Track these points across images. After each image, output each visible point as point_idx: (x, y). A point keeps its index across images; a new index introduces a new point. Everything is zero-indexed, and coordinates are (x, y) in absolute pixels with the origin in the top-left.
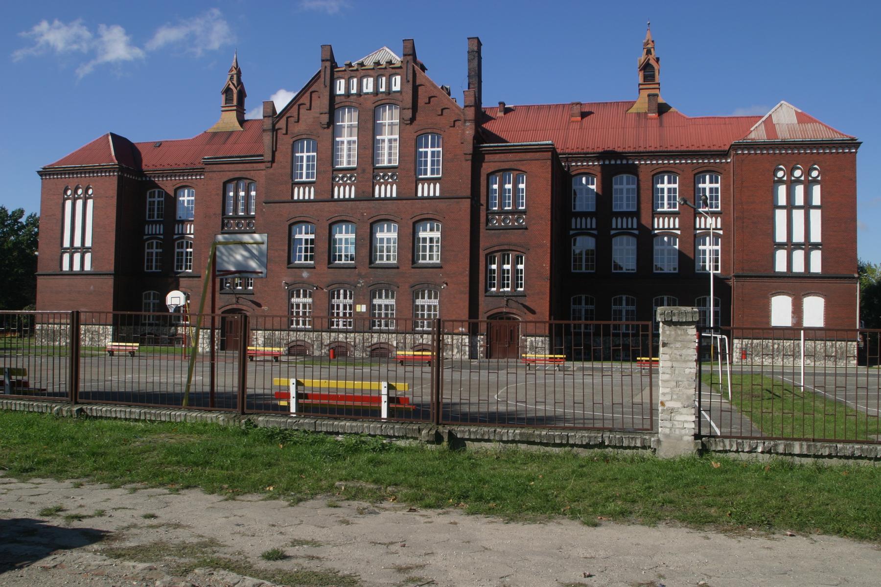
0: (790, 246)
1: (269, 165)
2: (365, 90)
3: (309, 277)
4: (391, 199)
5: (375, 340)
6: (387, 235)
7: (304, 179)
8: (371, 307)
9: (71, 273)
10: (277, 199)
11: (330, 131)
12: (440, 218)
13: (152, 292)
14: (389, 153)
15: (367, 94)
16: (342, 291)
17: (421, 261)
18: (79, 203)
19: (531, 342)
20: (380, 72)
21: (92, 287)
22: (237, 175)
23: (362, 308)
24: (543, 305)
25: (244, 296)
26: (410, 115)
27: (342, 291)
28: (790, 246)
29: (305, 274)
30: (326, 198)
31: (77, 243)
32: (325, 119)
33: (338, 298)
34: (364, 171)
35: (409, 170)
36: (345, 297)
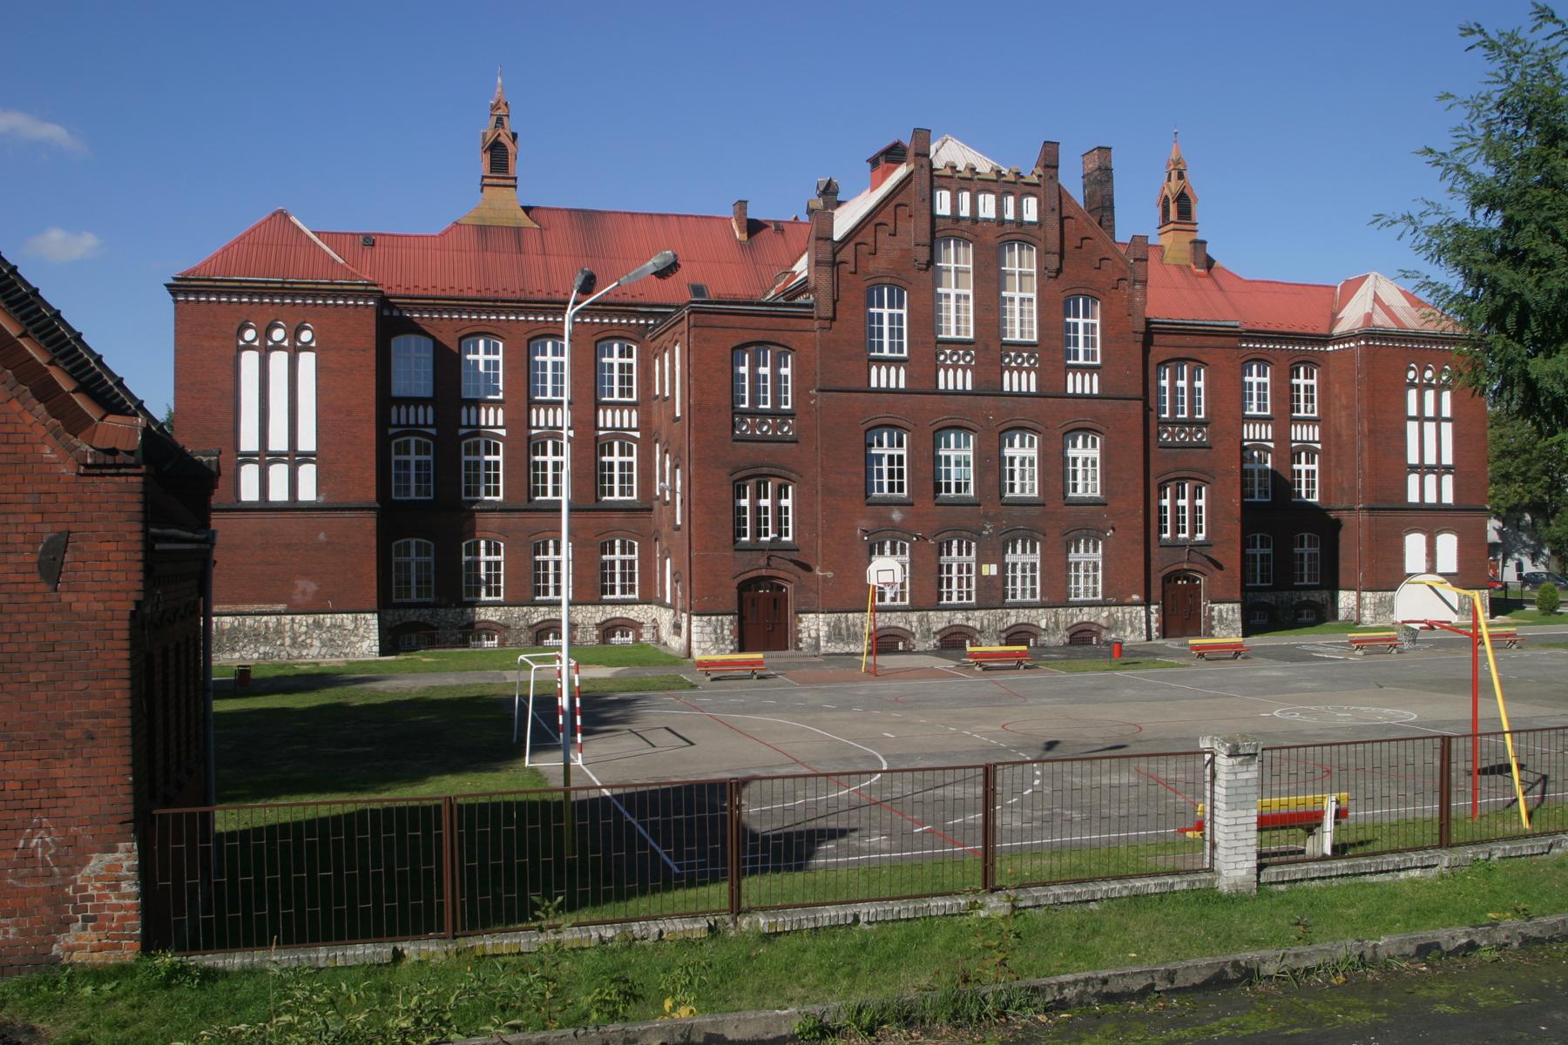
0: (1422, 469)
1: (827, 324)
2: (982, 215)
3: (903, 520)
4: (1028, 395)
5: (1013, 621)
6: (1022, 452)
7: (886, 353)
8: (1003, 568)
9: (264, 506)
10: (842, 384)
11: (927, 276)
12: (1103, 429)
13: (413, 541)
14: (1022, 323)
15: (987, 220)
16: (955, 543)
17: (1071, 494)
18: (279, 360)
19: (1220, 611)
20: (1008, 188)
21: (322, 536)
22: (759, 336)
23: (991, 570)
24: (1231, 556)
25: (780, 554)
26: (1056, 265)
27: (955, 543)
28: (1422, 469)
29: (896, 515)
30: (923, 385)
31: (279, 442)
32: (923, 254)
33: (949, 553)
34: (987, 347)
35: (1052, 350)
36: (960, 553)
